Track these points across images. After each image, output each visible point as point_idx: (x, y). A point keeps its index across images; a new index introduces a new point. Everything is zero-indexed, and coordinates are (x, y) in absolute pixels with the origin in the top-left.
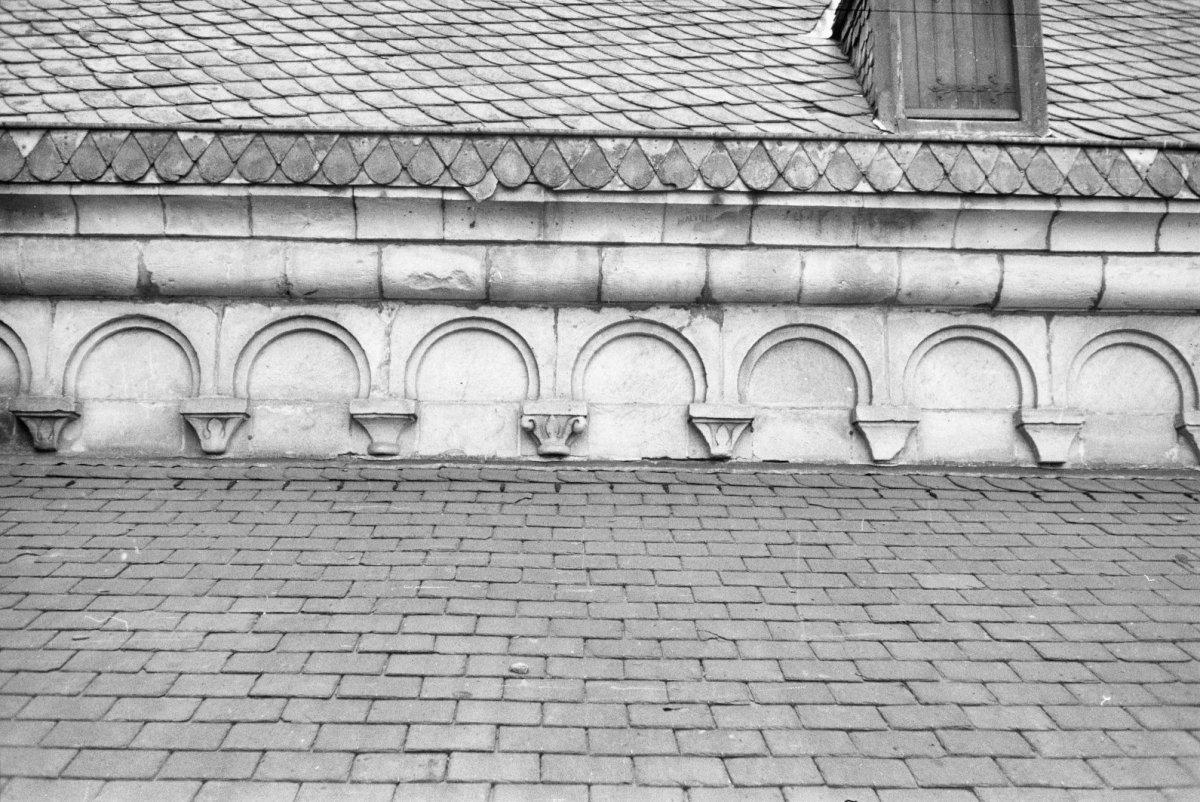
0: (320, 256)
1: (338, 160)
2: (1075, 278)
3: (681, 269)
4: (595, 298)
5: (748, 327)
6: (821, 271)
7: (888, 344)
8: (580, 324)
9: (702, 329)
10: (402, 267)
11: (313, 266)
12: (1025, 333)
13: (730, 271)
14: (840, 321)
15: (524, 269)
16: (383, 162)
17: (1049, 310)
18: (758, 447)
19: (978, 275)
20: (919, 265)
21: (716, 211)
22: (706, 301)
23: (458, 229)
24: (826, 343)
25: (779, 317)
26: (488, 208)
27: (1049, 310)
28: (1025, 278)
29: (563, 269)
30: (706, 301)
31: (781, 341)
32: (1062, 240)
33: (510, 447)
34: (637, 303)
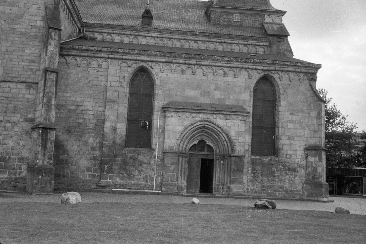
0: (110, 31)
1: (111, 26)
2: (150, 35)
3: (129, 33)
4: (125, 34)
5: (133, 36)
6: (136, 34)
7: (140, 38)
8: (124, 36)
9: (130, 37)
10: (115, 32)
11: (110, 31)
12: (148, 38)
13: (132, 33)
14: (138, 36)
15: (121, 32)
16: (114, 26)
17: (149, 37)
18: (133, 43)
19: (145, 34)
20: (141, 34)
21: (131, 30)
22: (131, 35)
23: (118, 30)
24: (137, 37)
25: (134, 36)
26: (120, 29)
27: (149, 37)
28: (147, 35)
29: (123, 33)
30: (131, 35)
31: (135, 37)
32: (149, 33)
33: (120, 42)
34: (127, 35)
